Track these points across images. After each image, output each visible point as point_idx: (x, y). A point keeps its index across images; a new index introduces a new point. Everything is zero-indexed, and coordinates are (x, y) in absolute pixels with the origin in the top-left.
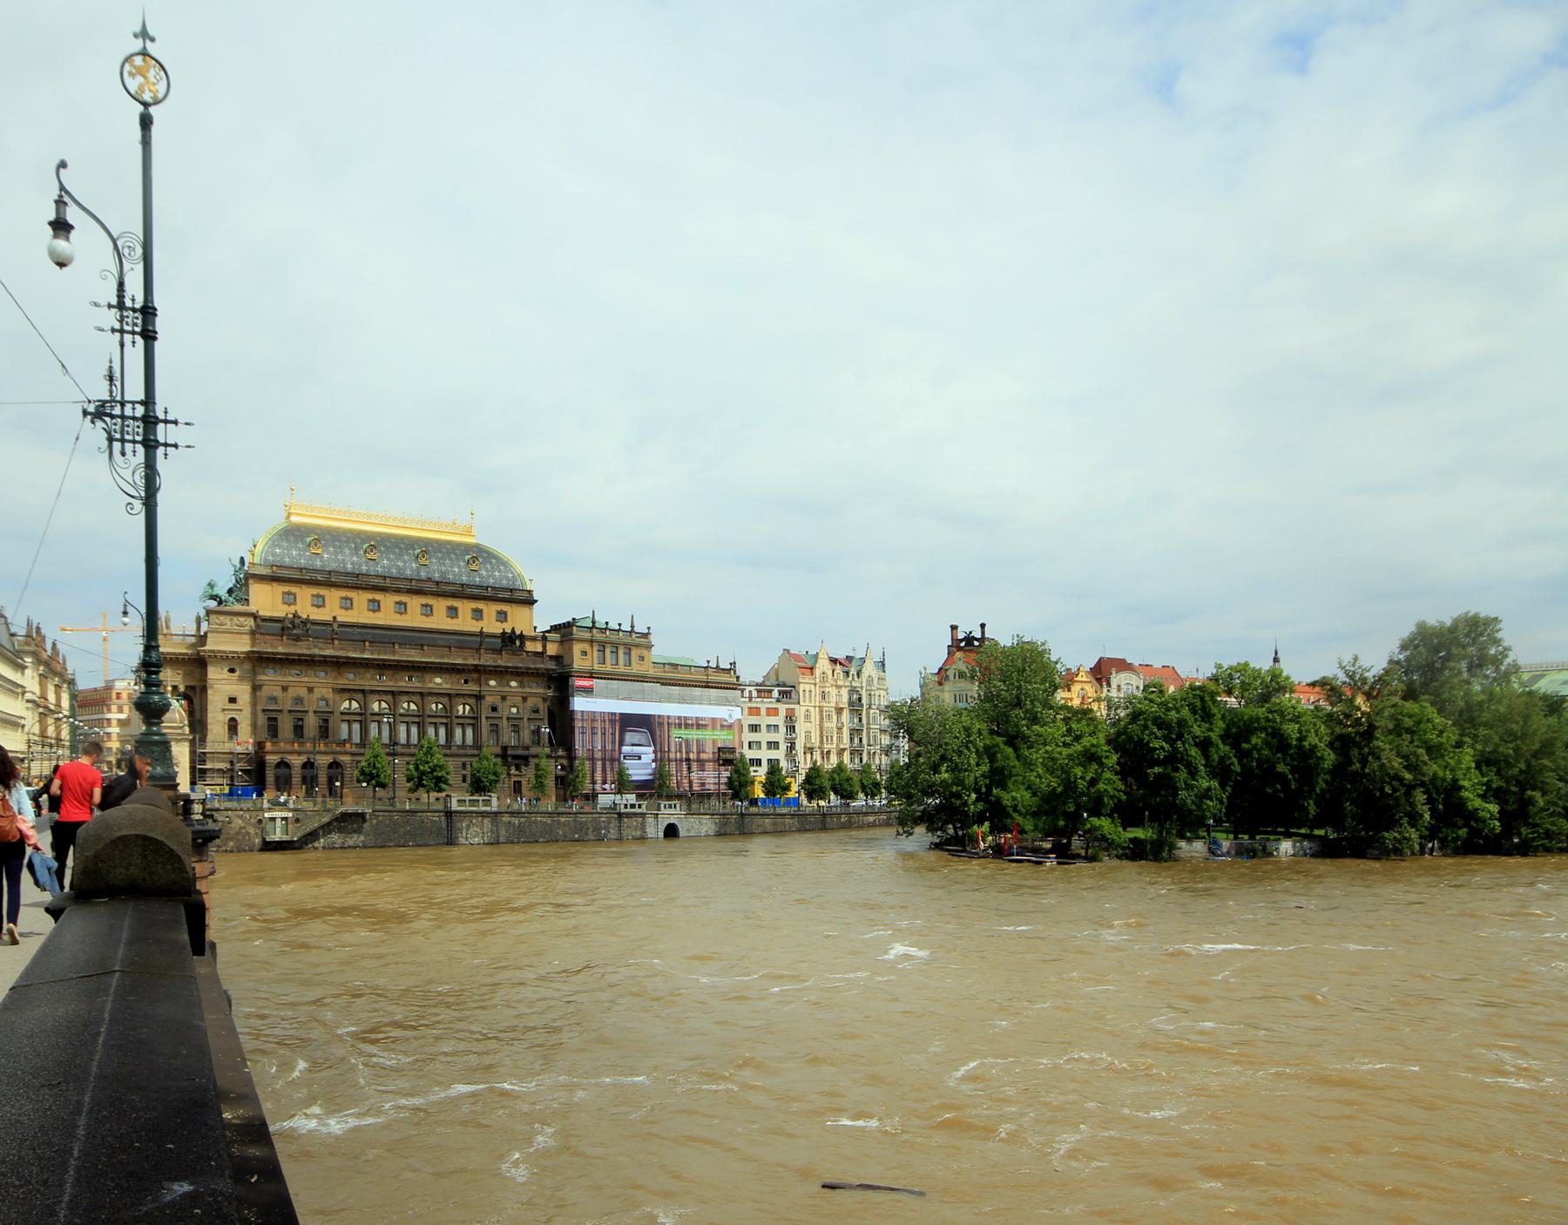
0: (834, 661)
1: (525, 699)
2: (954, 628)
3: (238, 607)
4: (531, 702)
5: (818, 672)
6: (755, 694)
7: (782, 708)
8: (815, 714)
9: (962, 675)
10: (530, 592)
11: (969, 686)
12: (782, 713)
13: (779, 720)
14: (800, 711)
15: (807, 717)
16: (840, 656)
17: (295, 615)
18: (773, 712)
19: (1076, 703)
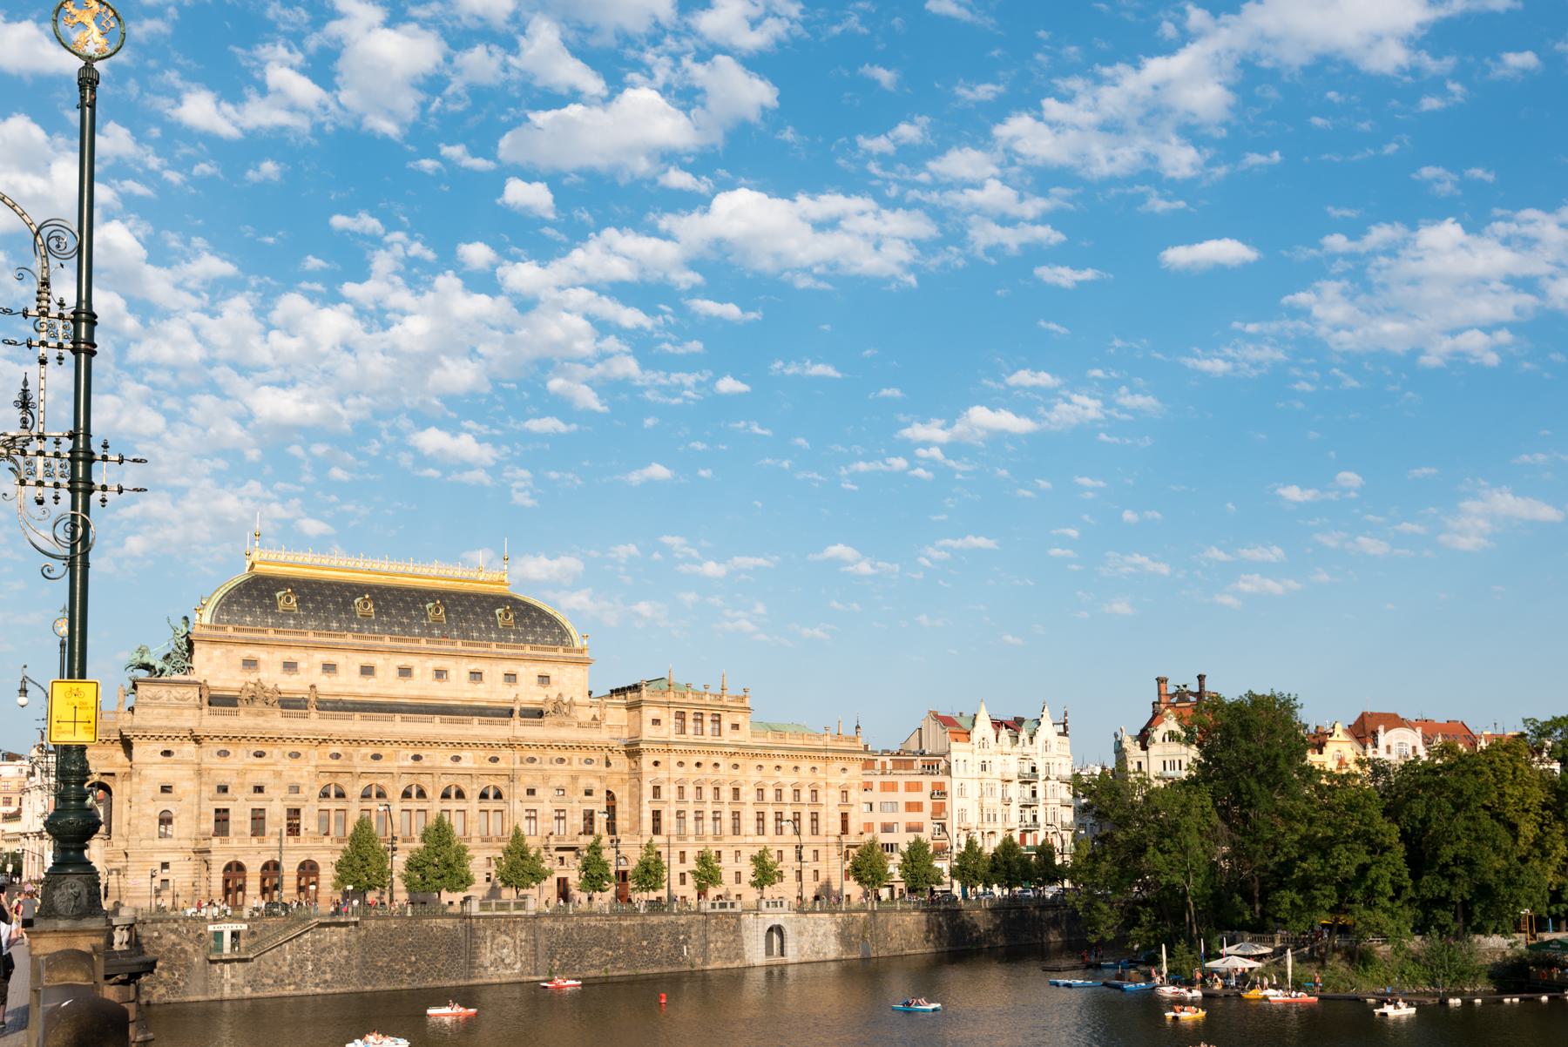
1: (574, 778)
2: (1161, 681)
3: (177, 677)
5: (976, 735)
6: (889, 765)
7: (927, 781)
8: (973, 789)
9: (1173, 736)
11: (1184, 749)
12: (927, 789)
13: (923, 797)
14: (952, 785)
15: (961, 791)
16: (1008, 716)
17: (258, 683)
18: (917, 787)
19: (1331, 765)
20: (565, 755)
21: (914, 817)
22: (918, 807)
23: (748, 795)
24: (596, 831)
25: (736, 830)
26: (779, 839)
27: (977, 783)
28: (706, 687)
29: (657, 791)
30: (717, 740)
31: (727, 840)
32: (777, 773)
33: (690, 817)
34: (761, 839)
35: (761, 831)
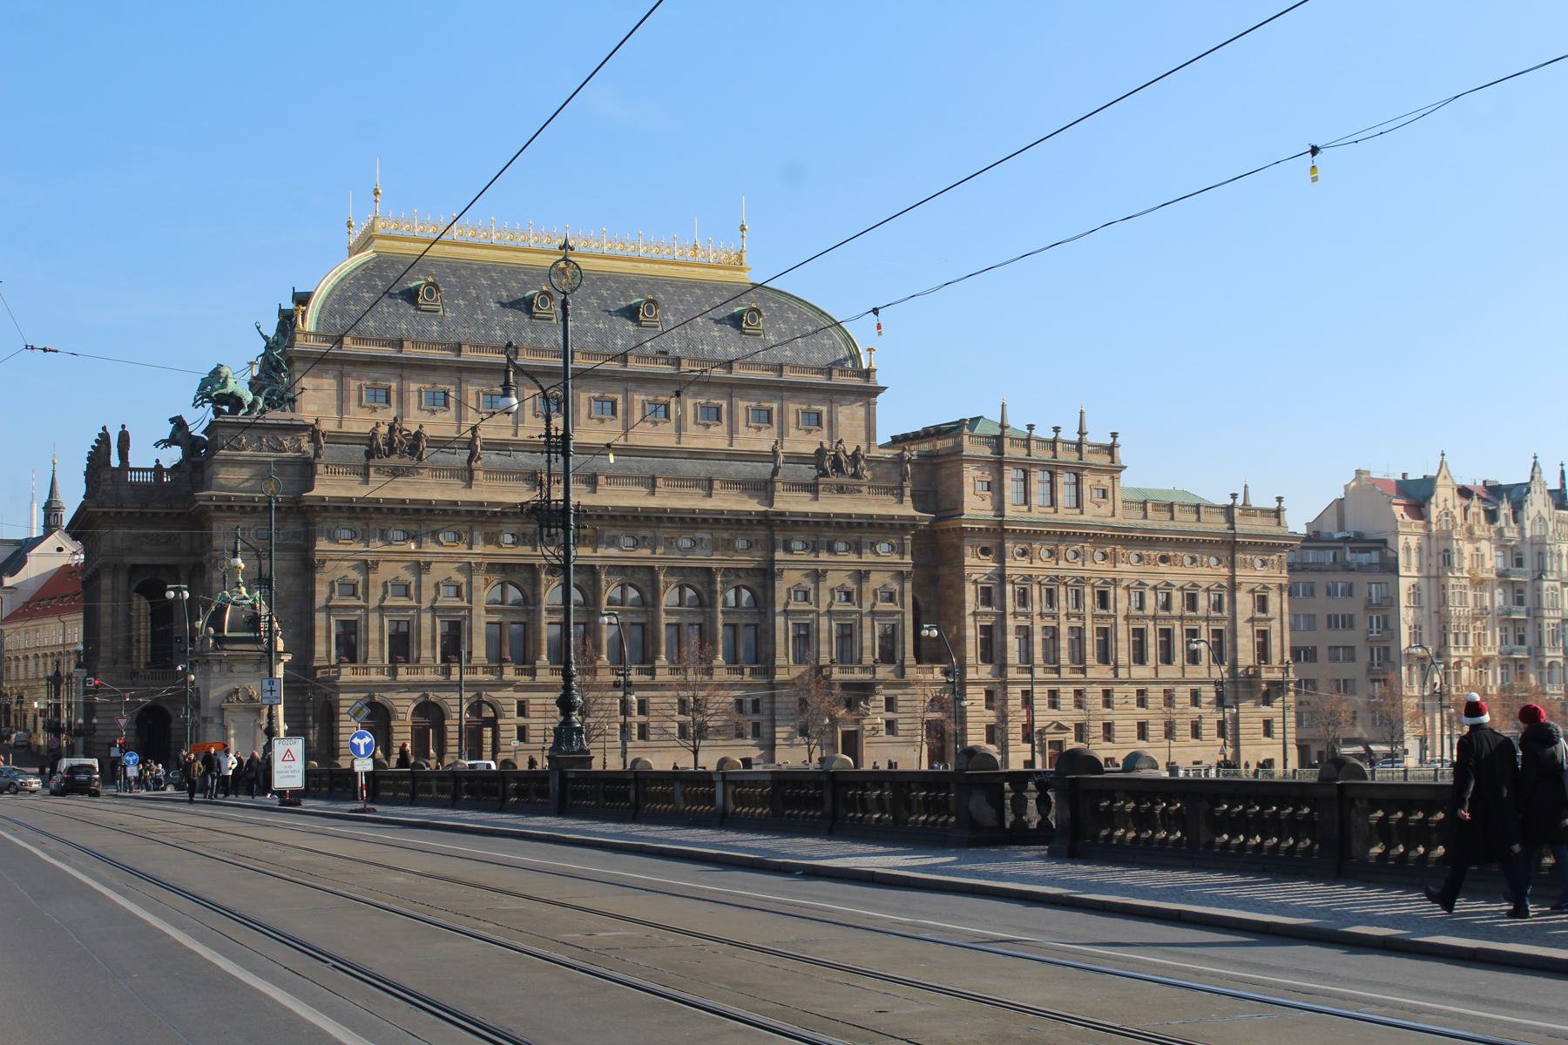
0: (1465, 492)
3: (275, 416)
4: (877, 580)
5: (1434, 512)
10: (867, 374)
20: (854, 536)
21: (1342, 637)
22: (1348, 622)
23: (1122, 602)
24: (898, 656)
25: (1104, 657)
26: (1193, 672)
27: (1433, 581)
28: (1057, 429)
29: (986, 596)
30: (1074, 516)
31: (1091, 674)
32: (1163, 567)
33: (1038, 638)
34: (1139, 672)
35: (1140, 658)
